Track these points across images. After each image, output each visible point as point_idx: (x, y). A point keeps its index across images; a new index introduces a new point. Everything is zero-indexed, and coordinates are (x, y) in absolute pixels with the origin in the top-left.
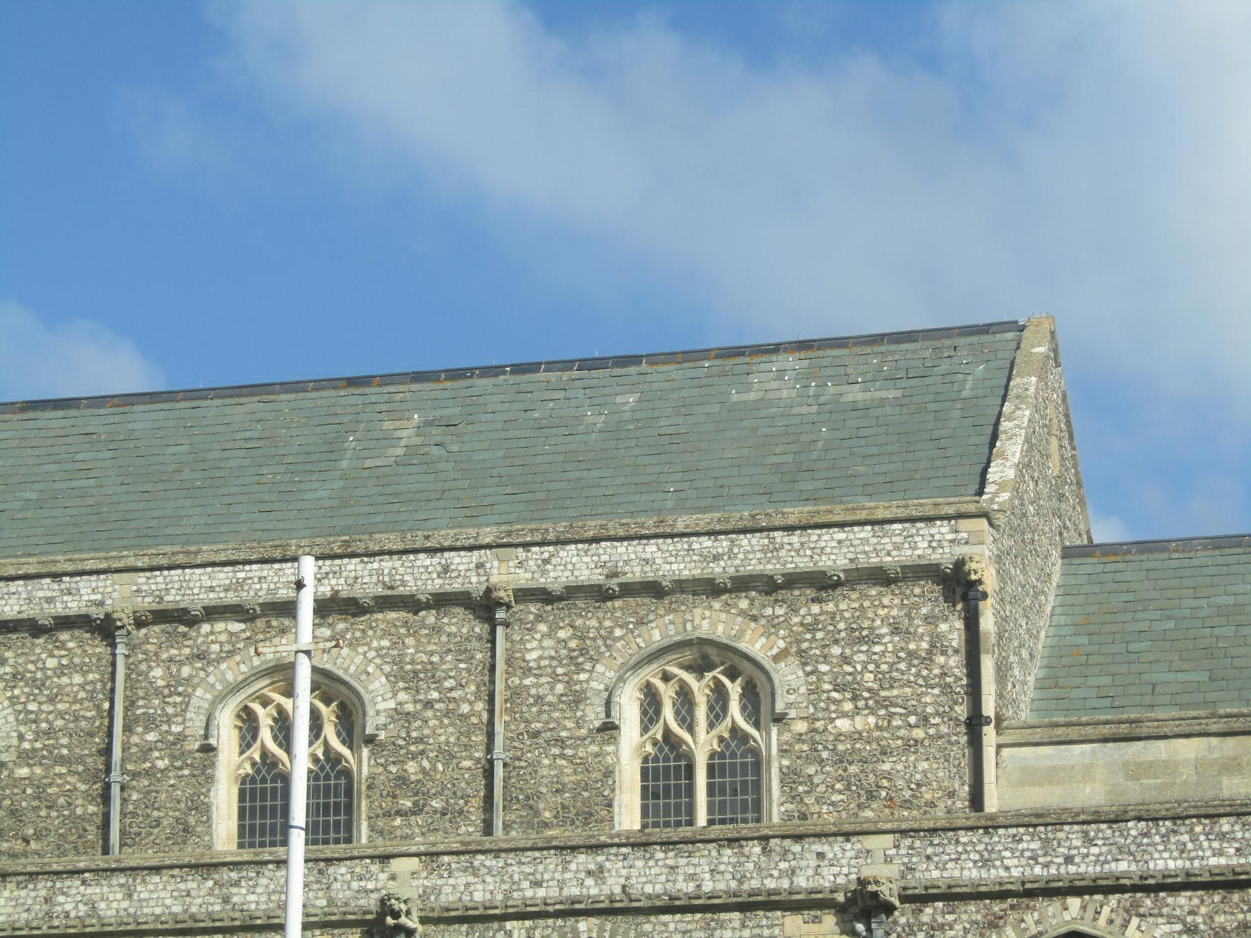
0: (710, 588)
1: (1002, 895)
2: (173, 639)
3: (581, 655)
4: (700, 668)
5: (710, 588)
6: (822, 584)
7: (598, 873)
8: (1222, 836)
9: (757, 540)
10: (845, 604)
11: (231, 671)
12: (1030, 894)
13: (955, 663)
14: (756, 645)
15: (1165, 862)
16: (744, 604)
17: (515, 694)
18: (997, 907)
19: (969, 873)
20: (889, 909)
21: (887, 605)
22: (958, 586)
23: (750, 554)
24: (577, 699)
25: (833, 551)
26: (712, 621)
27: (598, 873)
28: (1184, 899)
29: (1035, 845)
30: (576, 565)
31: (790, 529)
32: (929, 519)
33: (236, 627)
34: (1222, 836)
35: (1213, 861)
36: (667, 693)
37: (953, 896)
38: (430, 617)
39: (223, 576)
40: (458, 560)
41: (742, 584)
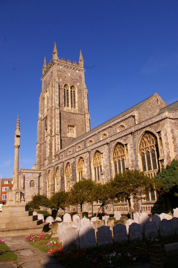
0: (121, 121)
1: (114, 140)
2: (99, 134)
3: (116, 129)
4: (122, 127)
5: (121, 121)
6: (126, 119)
7: (97, 145)
8: (125, 132)
9: (123, 117)
10: (128, 120)
11: (102, 135)
12: (116, 140)
13: (134, 122)
14: (124, 125)
15: (122, 135)
16: (123, 122)
17: (113, 132)
18: (114, 141)
19: (113, 139)
20: (109, 143)
21: (130, 119)
22: (134, 117)
23: (123, 118)
24: (116, 131)
25: (127, 116)
26: (122, 124)
27: (97, 145)
28: (123, 138)
29: (116, 136)
30: (115, 122)
31: (125, 116)
32: (131, 112)
33: (101, 132)
34: (125, 132)
35: (125, 134)
36: (120, 129)
37: (112, 141)
38: (109, 128)
39: (101, 129)
40: (110, 124)
41: (123, 120)
